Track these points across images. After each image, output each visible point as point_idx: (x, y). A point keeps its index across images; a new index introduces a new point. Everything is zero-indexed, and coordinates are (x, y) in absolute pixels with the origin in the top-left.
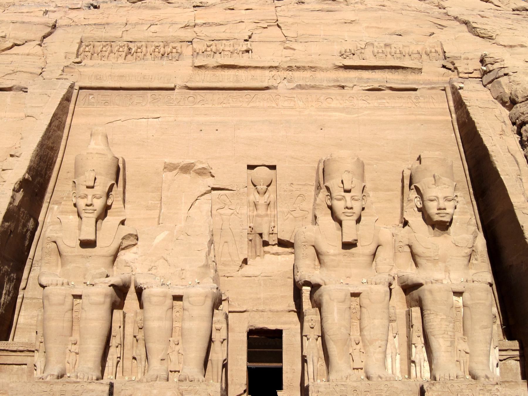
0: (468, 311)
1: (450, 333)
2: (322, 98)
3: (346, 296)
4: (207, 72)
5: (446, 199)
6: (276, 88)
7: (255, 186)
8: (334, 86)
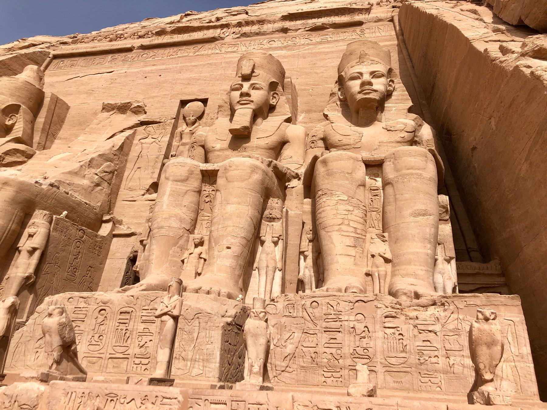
0: (389, 189)
1: (352, 224)
2: (265, 41)
3: (191, 173)
5: (374, 74)
6: (222, 39)
7: (184, 118)
8: (277, 31)
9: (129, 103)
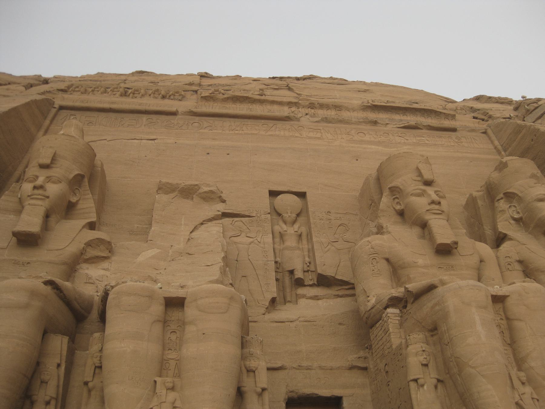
2: (353, 132)
4: (216, 104)
6: (298, 120)
9: (197, 185)
